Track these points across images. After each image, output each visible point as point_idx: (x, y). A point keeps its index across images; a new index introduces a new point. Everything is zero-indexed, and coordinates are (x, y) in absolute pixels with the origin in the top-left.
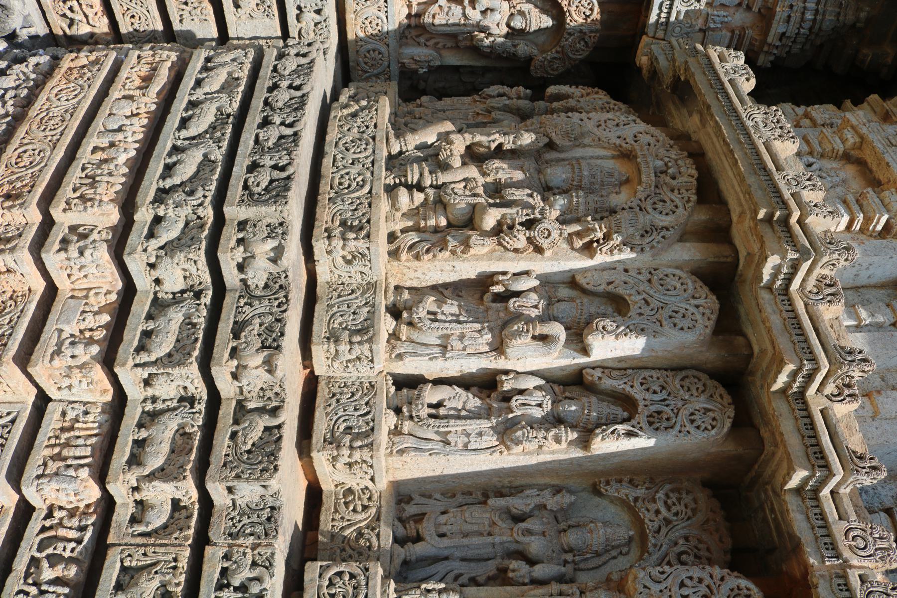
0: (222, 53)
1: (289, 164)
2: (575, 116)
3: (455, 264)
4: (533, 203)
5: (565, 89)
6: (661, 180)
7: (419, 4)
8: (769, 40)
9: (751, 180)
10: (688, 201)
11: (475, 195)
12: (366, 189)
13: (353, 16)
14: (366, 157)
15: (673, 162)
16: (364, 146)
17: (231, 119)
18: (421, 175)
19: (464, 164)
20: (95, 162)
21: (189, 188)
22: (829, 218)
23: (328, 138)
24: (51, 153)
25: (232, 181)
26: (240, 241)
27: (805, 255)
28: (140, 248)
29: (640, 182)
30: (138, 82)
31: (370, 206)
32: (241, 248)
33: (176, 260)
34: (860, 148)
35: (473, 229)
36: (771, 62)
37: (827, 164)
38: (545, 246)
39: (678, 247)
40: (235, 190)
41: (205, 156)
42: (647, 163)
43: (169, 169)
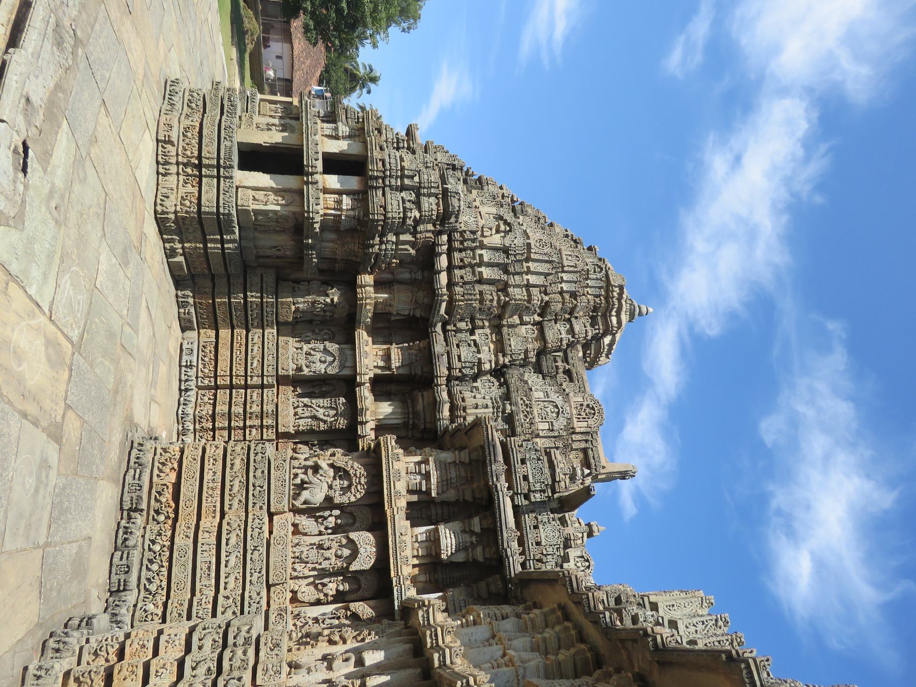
27: (429, 607)
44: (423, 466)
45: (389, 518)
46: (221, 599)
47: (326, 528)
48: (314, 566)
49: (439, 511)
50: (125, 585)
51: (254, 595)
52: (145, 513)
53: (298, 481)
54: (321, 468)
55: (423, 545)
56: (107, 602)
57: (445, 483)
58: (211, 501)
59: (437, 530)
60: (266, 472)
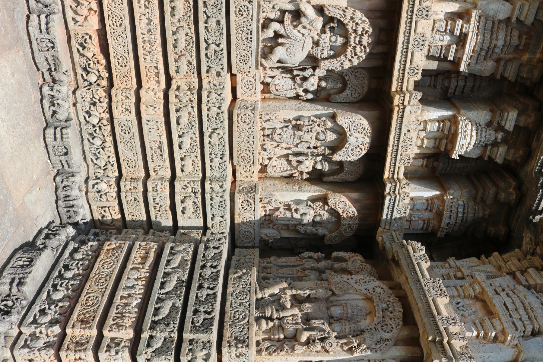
0: (179, 245)
1: (212, 311)
2: (346, 277)
3: (288, 357)
4: (324, 328)
5: (341, 254)
6: (386, 314)
7: (270, 210)
8: (442, 226)
9: (426, 320)
10: (398, 325)
11: (297, 324)
12: (246, 320)
13: (238, 216)
14: (246, 302)
15: (391, 304)
16: (245, 296)
17: (184, 284)
18: (272, 312)
19: (292, 305)
20: (122, 304)
21: (166, 321)
22: (462, 341)
23: (228, 291)
24: (102, 299)
25: (187, 320)
26: (190, 350)
28: (144, 352)
29: (375, 316)
30: (140, 260)
31: (248, 330)
32: (191, 354)
33: (160, 359)
34: (482, 294)
35: (296, 340)
36: (444, 235)
37: (468, 302)
38: (330, 350)
39: (394, 348)
40: (188, 325)
41: (173, 304)
42: (378, 306)
43: (157, 311)
44: (460, 23)
45: (396, 109)
46: (178, 186)
47: (306, 91)
48: (288, 146)
49: (461, 83)
50: (68, 164)
51: (216, 186)
52: (71, 72)
53: (270, 33)
54: (304, 15)
55: (431, 135)
56: (55, 182)
57: (483, 53)
58: (151, 60)
59: (454, 121)
60: (223, 22)
